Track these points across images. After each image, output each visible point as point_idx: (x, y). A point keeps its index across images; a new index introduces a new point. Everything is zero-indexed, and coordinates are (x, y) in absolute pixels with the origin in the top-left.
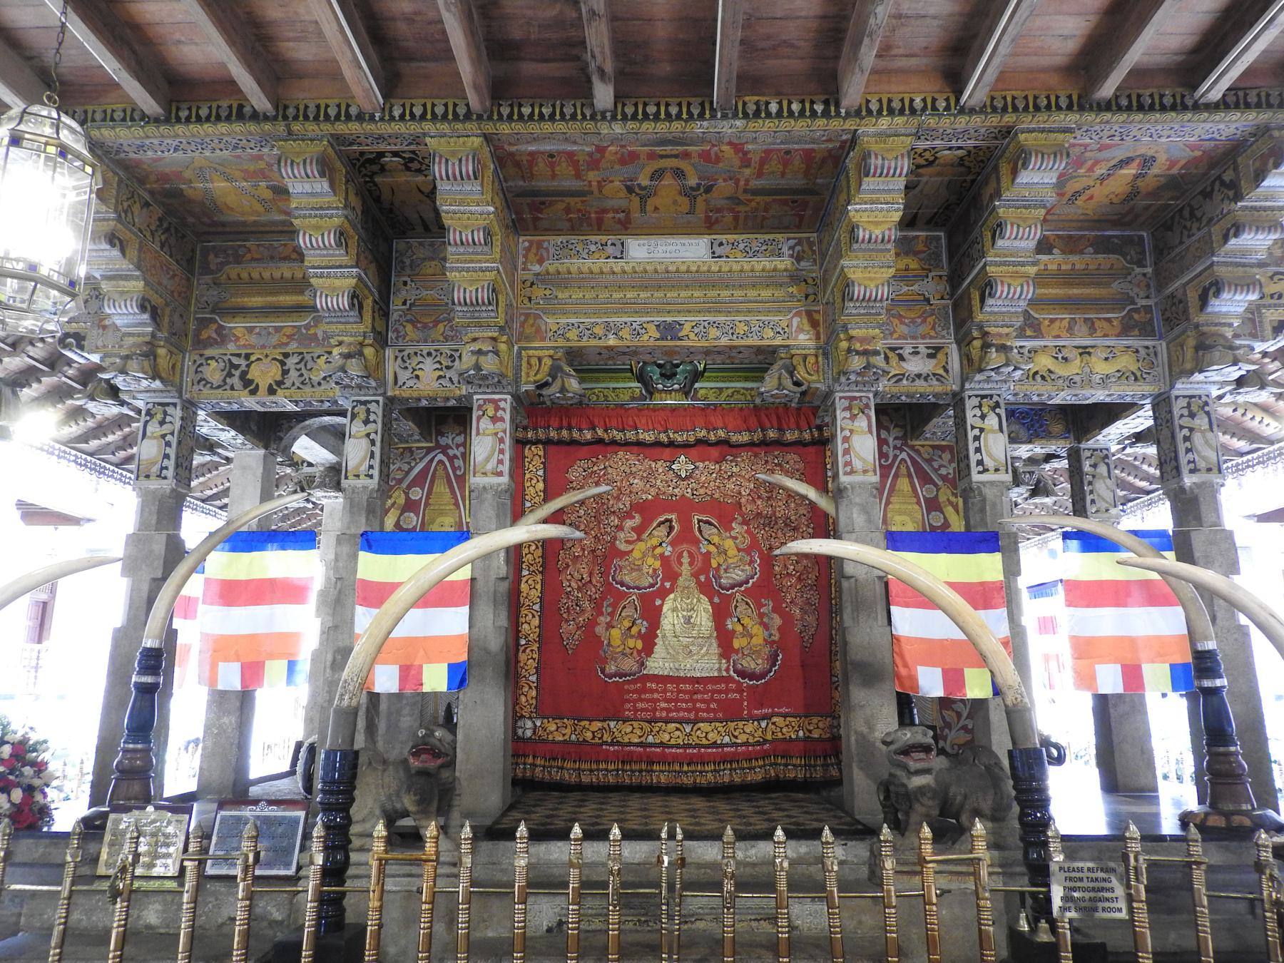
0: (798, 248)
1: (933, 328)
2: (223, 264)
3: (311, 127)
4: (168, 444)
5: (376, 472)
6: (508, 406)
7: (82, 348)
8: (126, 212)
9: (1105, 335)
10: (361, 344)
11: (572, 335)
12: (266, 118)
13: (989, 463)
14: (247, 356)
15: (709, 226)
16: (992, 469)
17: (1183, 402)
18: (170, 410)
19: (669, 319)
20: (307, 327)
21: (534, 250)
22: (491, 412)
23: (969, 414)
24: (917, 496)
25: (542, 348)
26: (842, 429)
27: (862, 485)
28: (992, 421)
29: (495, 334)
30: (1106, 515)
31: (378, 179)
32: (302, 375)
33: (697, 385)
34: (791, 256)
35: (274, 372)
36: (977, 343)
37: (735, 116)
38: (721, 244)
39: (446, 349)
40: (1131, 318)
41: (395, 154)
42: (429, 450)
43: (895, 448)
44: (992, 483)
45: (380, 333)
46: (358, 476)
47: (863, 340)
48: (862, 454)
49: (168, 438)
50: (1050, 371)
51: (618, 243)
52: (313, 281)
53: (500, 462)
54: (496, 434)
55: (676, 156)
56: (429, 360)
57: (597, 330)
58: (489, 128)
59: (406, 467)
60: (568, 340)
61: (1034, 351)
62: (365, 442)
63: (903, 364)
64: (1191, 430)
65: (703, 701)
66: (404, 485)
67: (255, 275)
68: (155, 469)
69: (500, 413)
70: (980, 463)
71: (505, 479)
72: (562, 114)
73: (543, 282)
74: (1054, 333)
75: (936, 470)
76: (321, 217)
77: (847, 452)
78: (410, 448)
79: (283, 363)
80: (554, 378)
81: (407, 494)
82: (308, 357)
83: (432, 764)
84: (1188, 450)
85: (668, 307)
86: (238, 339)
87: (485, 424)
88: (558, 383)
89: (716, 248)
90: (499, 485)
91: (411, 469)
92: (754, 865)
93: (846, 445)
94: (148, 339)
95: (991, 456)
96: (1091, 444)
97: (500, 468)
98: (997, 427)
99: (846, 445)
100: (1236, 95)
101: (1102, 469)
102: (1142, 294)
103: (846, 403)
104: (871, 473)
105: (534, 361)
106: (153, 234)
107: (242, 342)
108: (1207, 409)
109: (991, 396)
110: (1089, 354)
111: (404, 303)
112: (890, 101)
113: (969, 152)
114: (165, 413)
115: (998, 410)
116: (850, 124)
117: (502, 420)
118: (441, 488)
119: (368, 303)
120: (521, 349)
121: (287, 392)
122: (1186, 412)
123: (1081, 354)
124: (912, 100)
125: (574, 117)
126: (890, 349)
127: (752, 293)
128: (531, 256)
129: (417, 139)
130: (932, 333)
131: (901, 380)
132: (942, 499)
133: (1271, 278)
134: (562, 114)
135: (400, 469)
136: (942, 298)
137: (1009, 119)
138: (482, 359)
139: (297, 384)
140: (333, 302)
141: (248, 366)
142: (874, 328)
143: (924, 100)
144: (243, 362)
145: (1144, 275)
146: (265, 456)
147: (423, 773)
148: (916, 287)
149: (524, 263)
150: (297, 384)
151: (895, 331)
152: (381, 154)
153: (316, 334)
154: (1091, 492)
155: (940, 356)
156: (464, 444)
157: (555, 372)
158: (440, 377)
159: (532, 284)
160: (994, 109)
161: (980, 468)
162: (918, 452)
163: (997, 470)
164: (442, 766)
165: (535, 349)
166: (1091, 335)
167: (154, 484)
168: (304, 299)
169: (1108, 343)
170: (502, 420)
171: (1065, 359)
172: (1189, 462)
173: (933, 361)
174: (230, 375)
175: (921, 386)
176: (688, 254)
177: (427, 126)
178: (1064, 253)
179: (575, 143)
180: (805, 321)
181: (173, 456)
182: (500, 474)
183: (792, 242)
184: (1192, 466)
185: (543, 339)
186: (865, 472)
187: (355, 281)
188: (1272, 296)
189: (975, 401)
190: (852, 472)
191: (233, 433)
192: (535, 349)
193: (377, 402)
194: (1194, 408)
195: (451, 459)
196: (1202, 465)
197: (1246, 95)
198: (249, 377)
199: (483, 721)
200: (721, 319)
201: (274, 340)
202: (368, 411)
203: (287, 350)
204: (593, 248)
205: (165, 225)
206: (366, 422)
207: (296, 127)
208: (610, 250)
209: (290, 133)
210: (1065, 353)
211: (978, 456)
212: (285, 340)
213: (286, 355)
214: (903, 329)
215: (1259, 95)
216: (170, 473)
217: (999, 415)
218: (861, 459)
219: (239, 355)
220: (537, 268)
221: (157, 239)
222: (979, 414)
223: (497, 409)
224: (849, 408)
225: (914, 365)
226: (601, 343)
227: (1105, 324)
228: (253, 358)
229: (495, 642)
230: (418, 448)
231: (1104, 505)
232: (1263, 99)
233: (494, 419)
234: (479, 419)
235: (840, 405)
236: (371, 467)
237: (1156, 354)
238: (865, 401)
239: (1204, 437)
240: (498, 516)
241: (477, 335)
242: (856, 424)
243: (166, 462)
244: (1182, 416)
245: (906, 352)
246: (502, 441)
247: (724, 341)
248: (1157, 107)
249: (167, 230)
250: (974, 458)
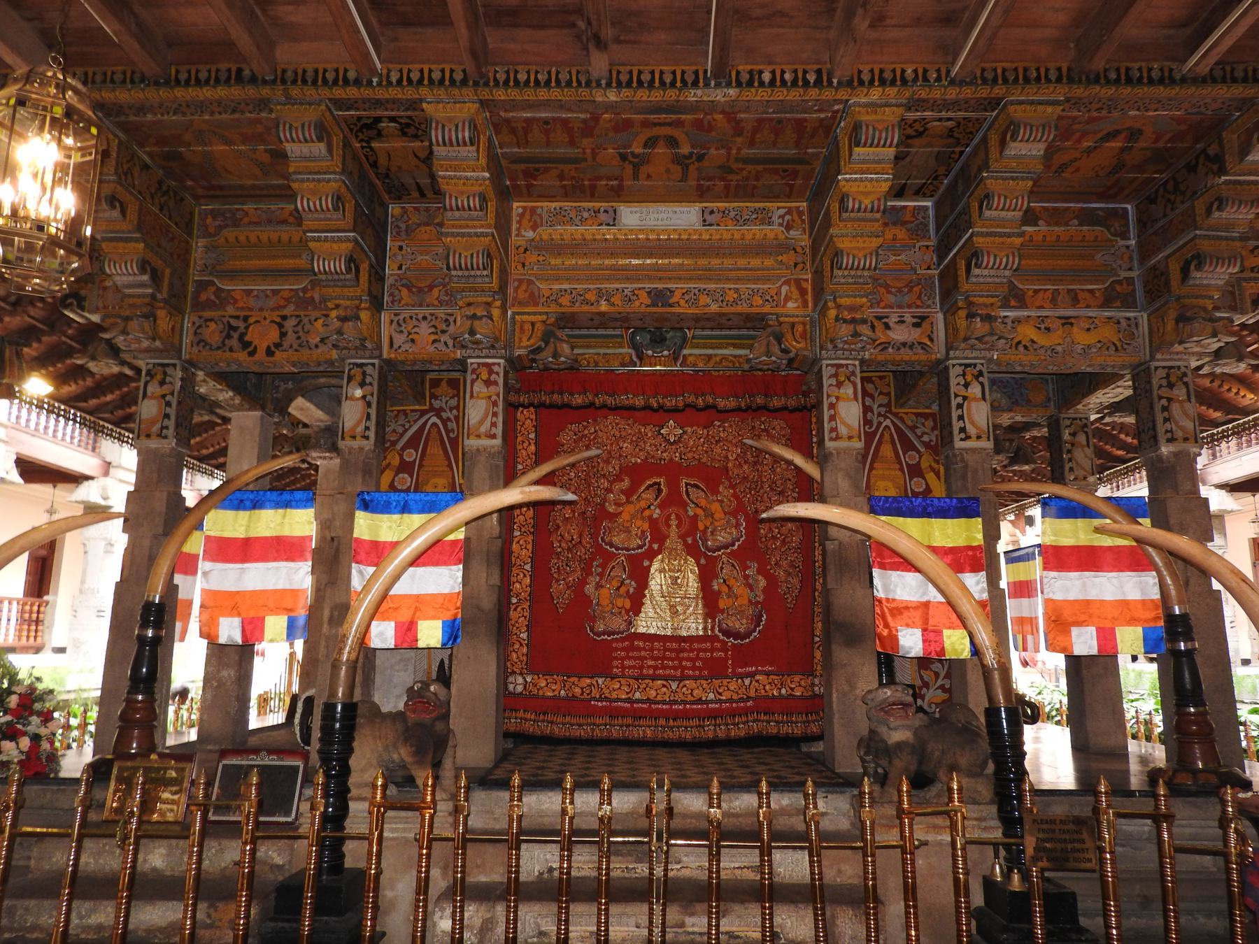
0: (787, 217)
1: (919, 297)
2: (220, 228)
3: (310, 92)
4: (168, 404)
5: (372, 434)
6: (501, 371)
7: (83, 309)
8: (126, 175)
9: (1088, 306)
10: (358, 308)
11: (565, 300)
12: (265, 82)
13: (972, 430)
14: (246, 319)
15: (702, 194)
16: (974, 436)
18: (169, 370)
19: (660, 286)
20: (305, 290)
21: (527, 216)
22: (484, 376)
23: (953, 382)
24: (900, 463)
25: (535, 314)
26: (828, 396)
27: (846, 451)
28: (975, 390)
29: (490, 299)
30: (1084, 483)
31: (375, 144)
32: (299, 338)
33: (685, 352)
34: (781, 225)
35: (274, 335)
36: (962, 313)
37: (729, 85)
38: (712, 212)
39: (441, 312)
40: (1114, 289)
41: (392, 119)
42: (423, 413)
43: (879, 415)
44: (974, 450)
45: (376, 297)
46: (354, 437)
47: (851, 309)
48: (847, 420)
49: (167, 398)
50: (1033, 341)
51: (611, 213)
52: (311, 244)
53: (494, 424)
54: (490, 397)
55: (670, 124)
56: (424, 324)
57: (591, 297)
58: (485, 94)
59: (400, 430)
60: (561, 305)
61: (1017, 321)
62: (360, 405)
63: (890, 333)
64: (1169, 400)
65: (689, 659)
66: (399, 446)
67: (253, 239)
68: (156, 428)
69: (493, 377)
70: (963, 430)
71: (498, 442)
72: (558, 81)
73: (536, 248)
74: (1038, 304)
75: (919, 437)
76: (319, 181)
77: (832, 418)
78: (404, 411)
79: (281, 326)
80: (547, 344)
81: (401, 456)
82: (306, 320)
83: (427, 718)
84: (1166, 420)
85: (660, 274)
86: (236, 301)
87: (479, 387)
88: (551, 348)
89: (707, 216)
90: (492, 447)
91: (406, 431)
92: (737, 816)
93: (832, 412)
94: (147, 300)
95: (973, 423)
96: (1071, 413)
97: (494, 430)
98: (980, 395)
99: (832, 412)
100: (1223, 69)
101: (1082, 438)
102: (1125, 266)
103: (833, 371)
104: (856, 439)
105: (528, 327)
106: (152, 197)
107: (241, 304)
108: (1185, 379)
109: (975, 365)
110: (1072, 324)
111: (400, 268)
112: (882, 71)
113: (959, 123)
114: (165, 374)
115: (981, 379)
116: (843, 94)
117: (496, 383)
118: (434, 450)
119: (365, 267)
120: (514, 314)
121: (285, 355)
122: (1164, 382)
123: (1063, 325)
124: (903, 71)
125: (569, 83)
126: (877, 317)
127: (742, 262)
128: (525, 221)
129: (414, 105)
130: (919, 303)
131: (886, 348)
132: (924, 465)
133: (1252, 251)
134: (558, 81)
135: (394, 431)
136: (929, 268)
137: (998, 91)
138: (477, 323)
139: (295, 346)
140: (330, 266)
141: (247, 328)
142: (861, 297)
143: (915, 71)
144: (242, 325)
145: (1128, 247)
146: (262, 417)
147: (420, 725)
148: (902, 257)
149: (518, 229)
150: (295, 346)
151: (881, 300)
152: (378, 120)
153: (313, 298)
154: (1070, 460)
155: (925, 325)
156: (457, 407)
157: (548, 337)
158: (434, 341)
159: (526, 250)
160: (984, 81)
161: (963, 436)
162: (902, 419)
163: (979, 437)
164: (437, 718)
165: (529, 314)
166: (1074, 306)
167: (154, 444)
168: (302, 262)
169: (1090, 314)
170: (496, 383)
171: (1048, 329)
172: (1167, 431)
173: (919, 330)
174: (229, 336)
175: (906, 354)
176: (679, 222)
177: (424, 91)
178: (1049, 224)
179: (570, 110)
180: (793, 289)
181: (173, 417)
182: (494, 437)
183: (782, 211)
184: (1169, 435)
185: (536, 304)
186: (850, 438)
187: (350, 245)
188: (1252, 270)
189: (959, 370)
190: (837, 438)
191: (231, 394)
192: (529, 314)
193: (373, 365)
194: (1173, 379)
195: (444, 422)
196: (1180, 434)
197: (1233, 70)
198: (247, 338)
199: (477, 676)
200: (712, 286)
201: (271, 303)
202: (364, 374)
203: (285, 312)
204: (586, 215)
205: (164, 188)
207: (295, 91)
208: (603, 217)
209: (288, 97)
210: (1048, 323)
212: (282, 303)
213: (284, 318)
214: (892, 299)
215: (1246, 70)
216: (171, 432)
217: (982, 384)
218: (847, 426)
219: (237, 317)
220: (530, 234)
221: (157, 201)
222: (963, 382)
223: (491, 372)
224: (836, 375)
225: (899, 334)
226: (594, 309)
227: (1087, 295)
228: (252, 320)
229: (488, 601)
230: (412, 411)
231: (1082, 473)
232: (1250, 74)
233: (488, 383)
234: (473, 382)
235: (827, 372)
236: (367, 428)
237: (1137, 325)
238: (851, 368)
239: (1182, 407)
240: (491, 478)
241: (472, 300)
243: (166, 422)
244: (1161, 386)
245: (893, 320)
246: (495, 404)
247: (714, 308)
248: (1145, 80)
249: (167, 192)
250: (956, 425)
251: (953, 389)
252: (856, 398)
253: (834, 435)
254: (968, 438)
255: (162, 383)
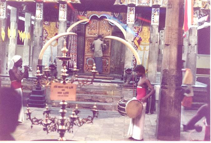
4: (4, 10)
28: (157, 13)
46: (38, 17)
49: (4, 8)
53: (65, 16)
70: (153, 21)
77: (129, 17)
87: (62, 8)
98: (157, 14)
117: (65, 8)
170: (65, 8)
182: (65, 18)
186: (132, 21)
190: (129, 21)
206: (40, 7)
211: (153, 20)
217: (158, 12)
236: (41, 16)
242: (131, 12)
243: (4, 13)
251: (152, 13)
252: (134, 14)
253: (129, 21)
254: (154, 22)
255: (3, 5)
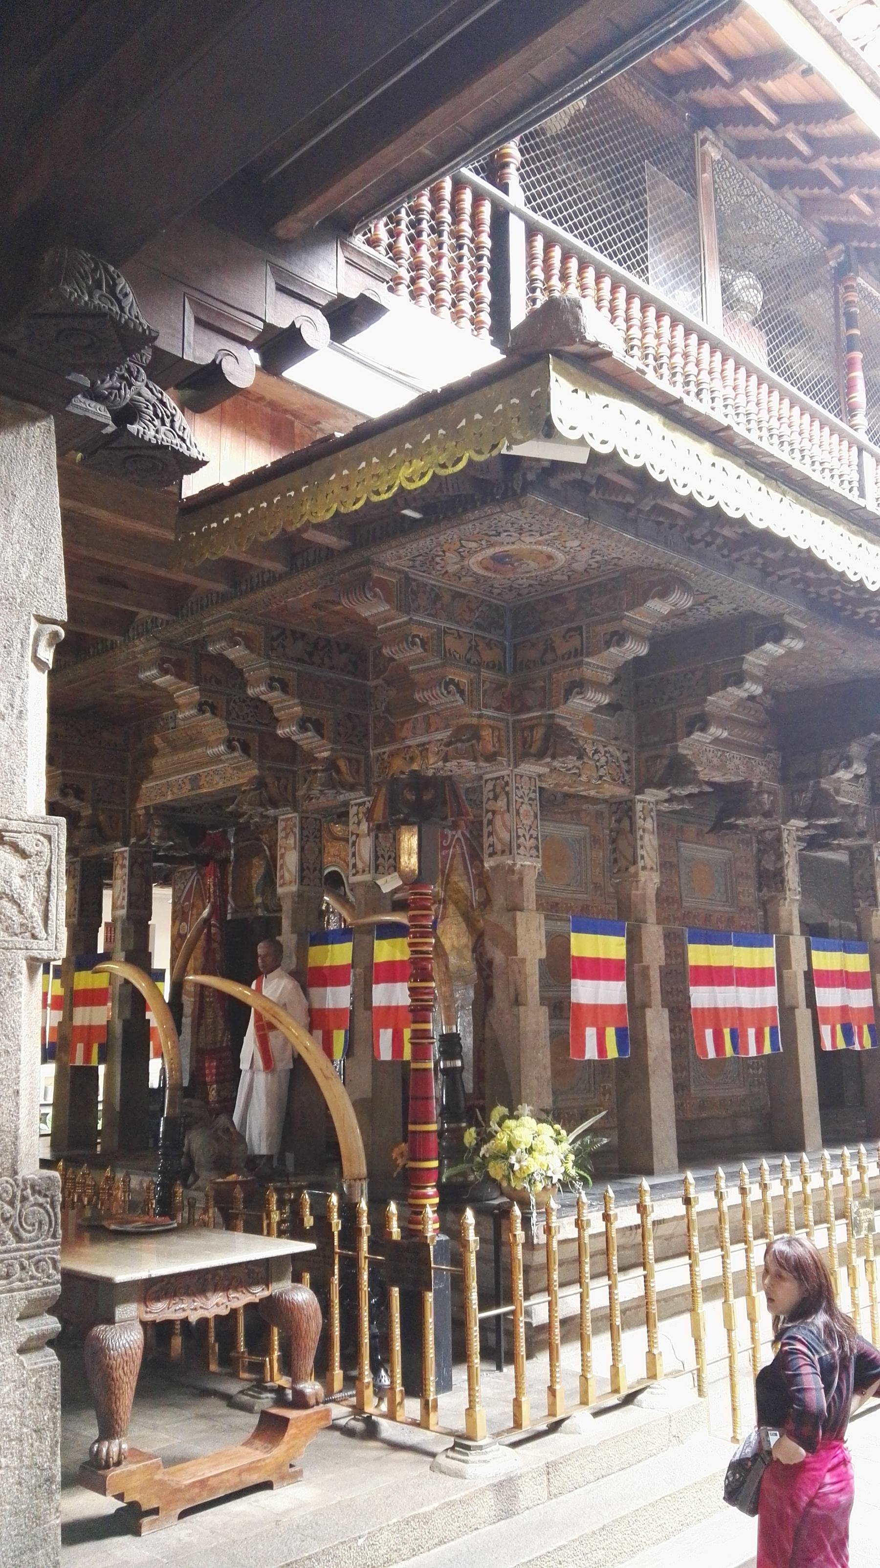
13: (360, 865)
17: (490, 786)
70: (354, 866)
84: (490, 834)
95: (361, 859)
122: (491, 795)
172: (490, 846)
194: (498, 790)
196: (499, 847)
239: (502, 818)
244: (489, 799)
